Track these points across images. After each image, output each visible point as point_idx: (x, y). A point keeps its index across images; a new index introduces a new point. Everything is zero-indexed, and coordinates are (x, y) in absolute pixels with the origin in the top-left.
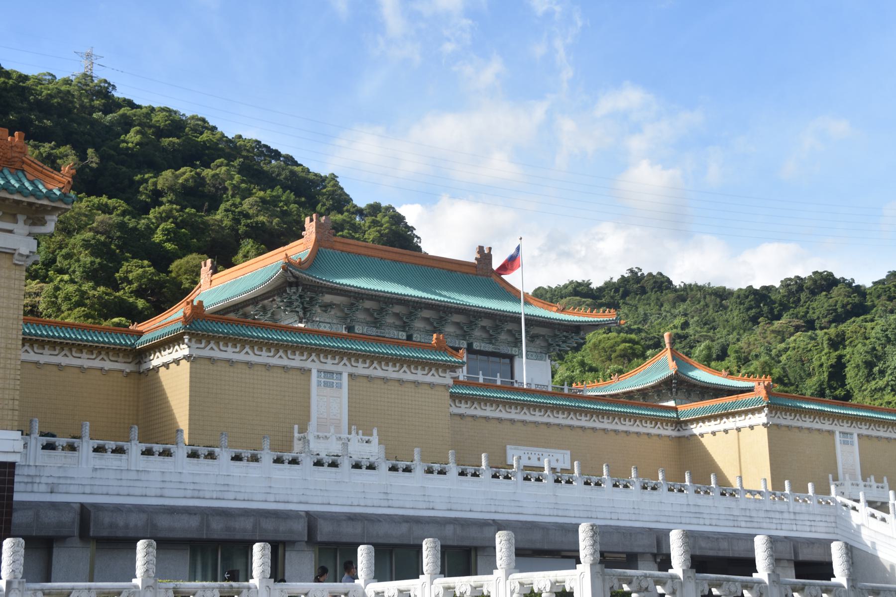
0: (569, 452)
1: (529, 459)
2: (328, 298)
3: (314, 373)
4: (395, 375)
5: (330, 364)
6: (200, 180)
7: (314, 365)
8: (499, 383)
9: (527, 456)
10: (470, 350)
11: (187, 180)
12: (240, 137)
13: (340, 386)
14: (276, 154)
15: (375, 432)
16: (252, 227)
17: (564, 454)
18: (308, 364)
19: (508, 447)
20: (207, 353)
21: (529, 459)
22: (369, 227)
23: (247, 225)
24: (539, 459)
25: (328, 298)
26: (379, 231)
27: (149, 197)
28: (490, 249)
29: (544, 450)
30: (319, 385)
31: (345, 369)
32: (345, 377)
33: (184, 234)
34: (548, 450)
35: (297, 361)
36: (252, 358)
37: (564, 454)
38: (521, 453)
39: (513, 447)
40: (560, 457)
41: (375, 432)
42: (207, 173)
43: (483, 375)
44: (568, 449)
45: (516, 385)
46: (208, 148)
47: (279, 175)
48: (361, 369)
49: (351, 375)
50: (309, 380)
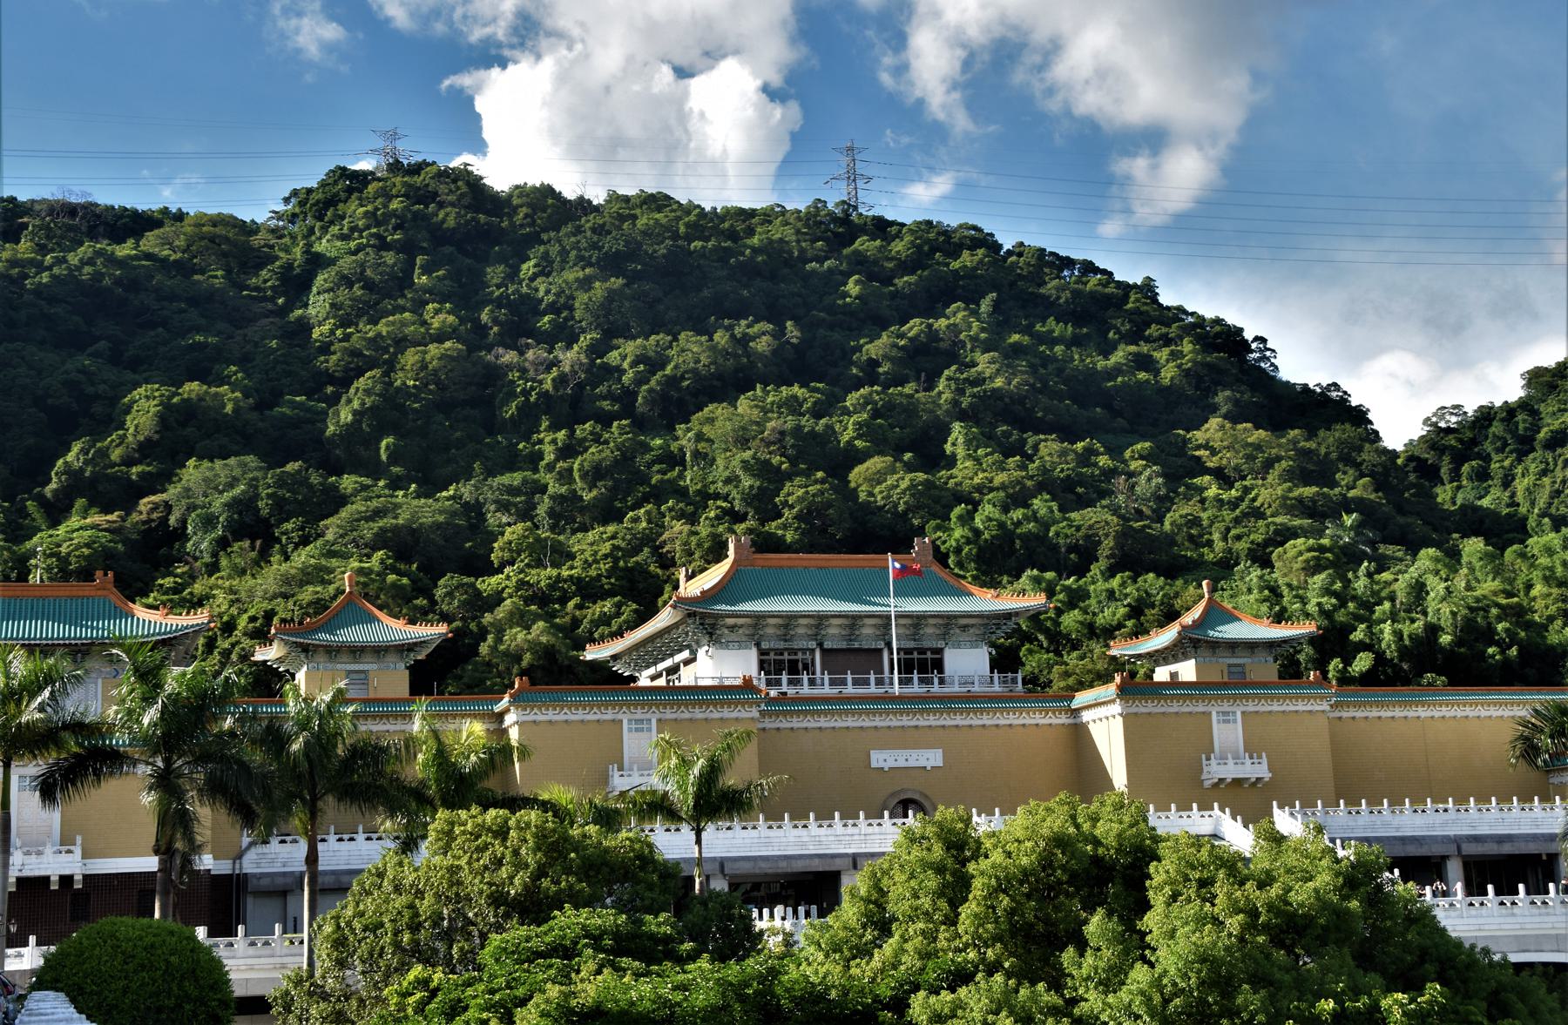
2: (730, 621)
3: (625, 722)
4: (701, 716)
6: (932, 334)
11: (918, 335)
12: (1021, 244)
14: (1068, 262)
16: (980, 397)
18: (620, 716)
22: (1168, 361)
23: (973, 396)
26: (1179, 367)
27: (862, 370)
30: (630, 730)
32: (654, 722)
33: (880, 426)
42: (942, 323)
46: (962, 278)
47: (1059, 298)
49: (659, 721)
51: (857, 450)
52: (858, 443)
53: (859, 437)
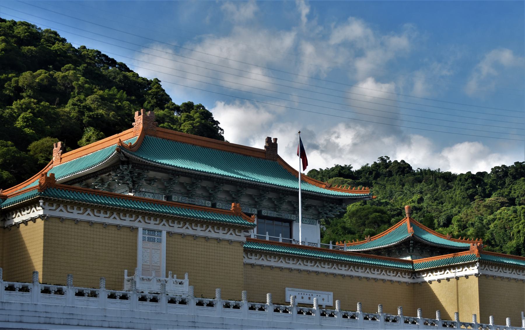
0: (332, 293)
1: (302, 298)
3: (140, 231)
4: (202, 234)
5: (152, 224)
7: (140, 225)
8: (281, 241)
9: (300, 296)
10: (260, 216)
13: (160, 241)
15: (186, 276)
16: (94, 118)
17: (328, 295)
18: (136, 224)
19: (287, 289)
20: (57, 213)
21: (302, 298)
22: (184, 121)
23: (90, 117)
24: (309, 298)
25: (152, 174)
26: (192, 124)
28: (276, 140)
29: (314, 291)
30: (144, 239)
31: (164, 228)
32: (164, 234)
34: (317, 292)
35: (127, 221)
36: (92, 218)
37: (328, 295)
38: (296, 294)
39: (290, 289)
40: (325, 297)
41: (186, 276)
43: (269, 235)
44: (332, 291)
45: (293, 243)
48: (176, 228)
49: (168, 233)
50: (136, 236)
51: (27, 135)
52: (27, 130)
53: (27, 126)
